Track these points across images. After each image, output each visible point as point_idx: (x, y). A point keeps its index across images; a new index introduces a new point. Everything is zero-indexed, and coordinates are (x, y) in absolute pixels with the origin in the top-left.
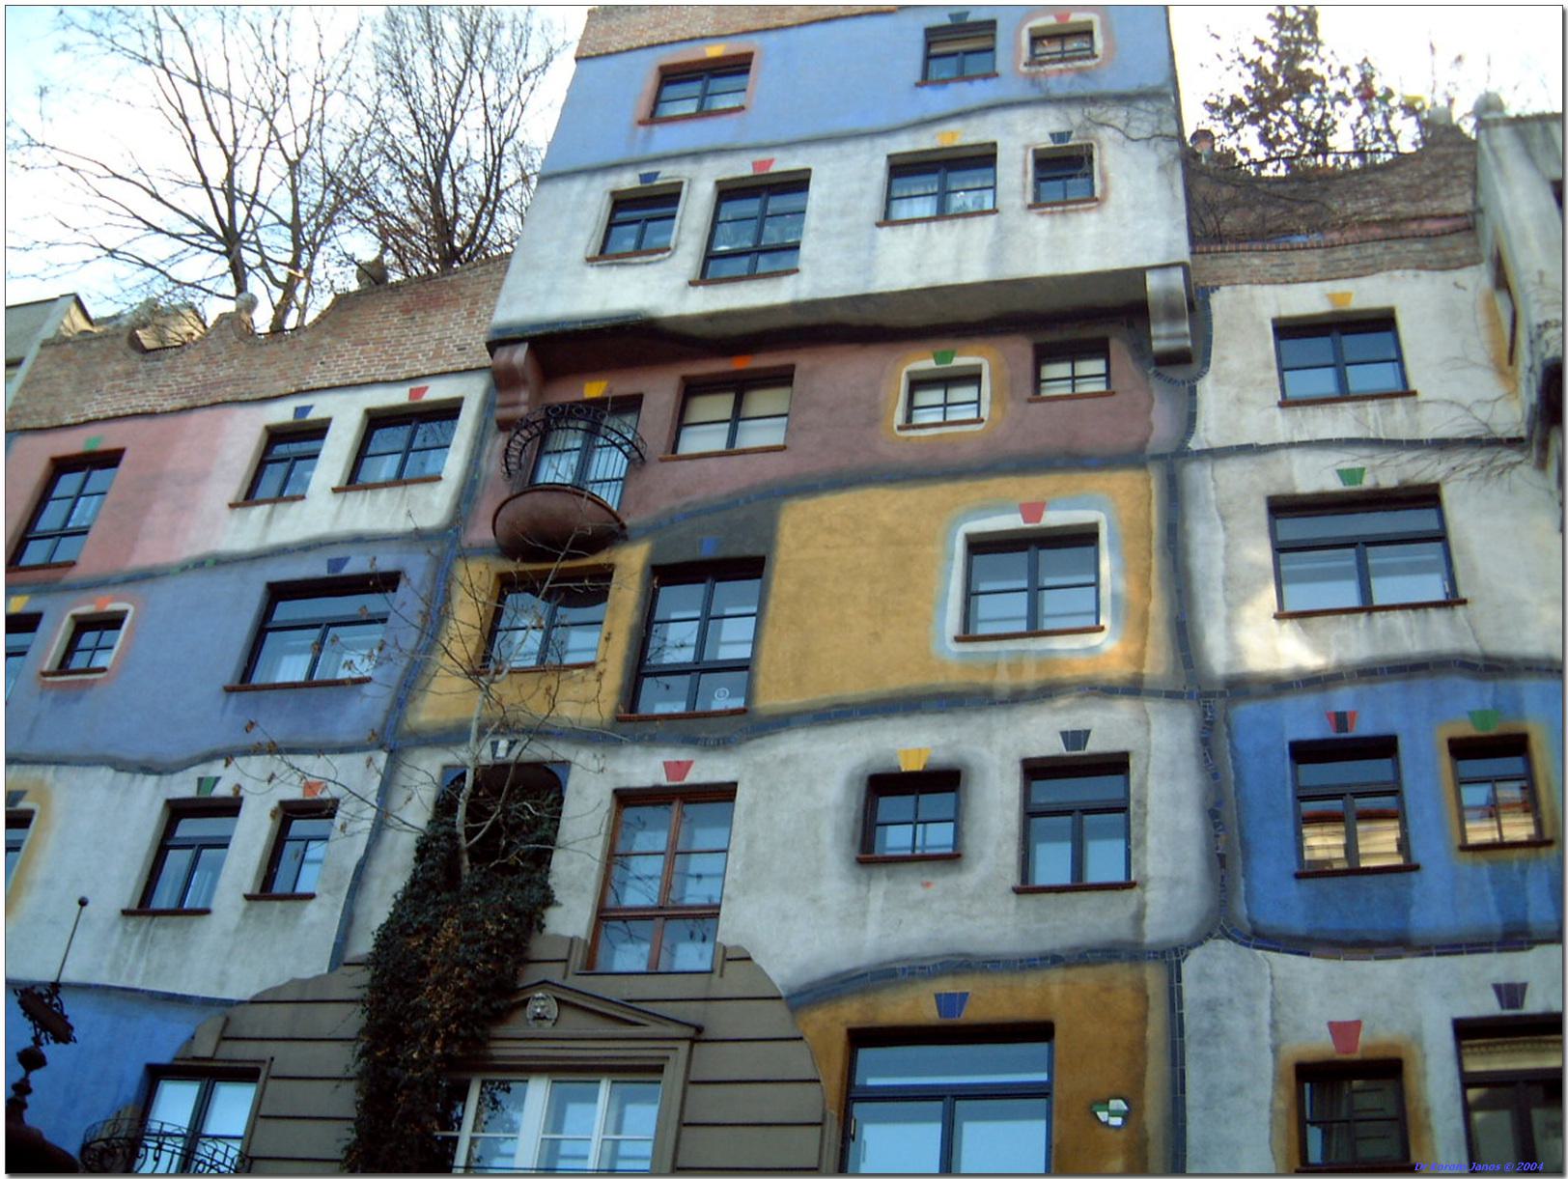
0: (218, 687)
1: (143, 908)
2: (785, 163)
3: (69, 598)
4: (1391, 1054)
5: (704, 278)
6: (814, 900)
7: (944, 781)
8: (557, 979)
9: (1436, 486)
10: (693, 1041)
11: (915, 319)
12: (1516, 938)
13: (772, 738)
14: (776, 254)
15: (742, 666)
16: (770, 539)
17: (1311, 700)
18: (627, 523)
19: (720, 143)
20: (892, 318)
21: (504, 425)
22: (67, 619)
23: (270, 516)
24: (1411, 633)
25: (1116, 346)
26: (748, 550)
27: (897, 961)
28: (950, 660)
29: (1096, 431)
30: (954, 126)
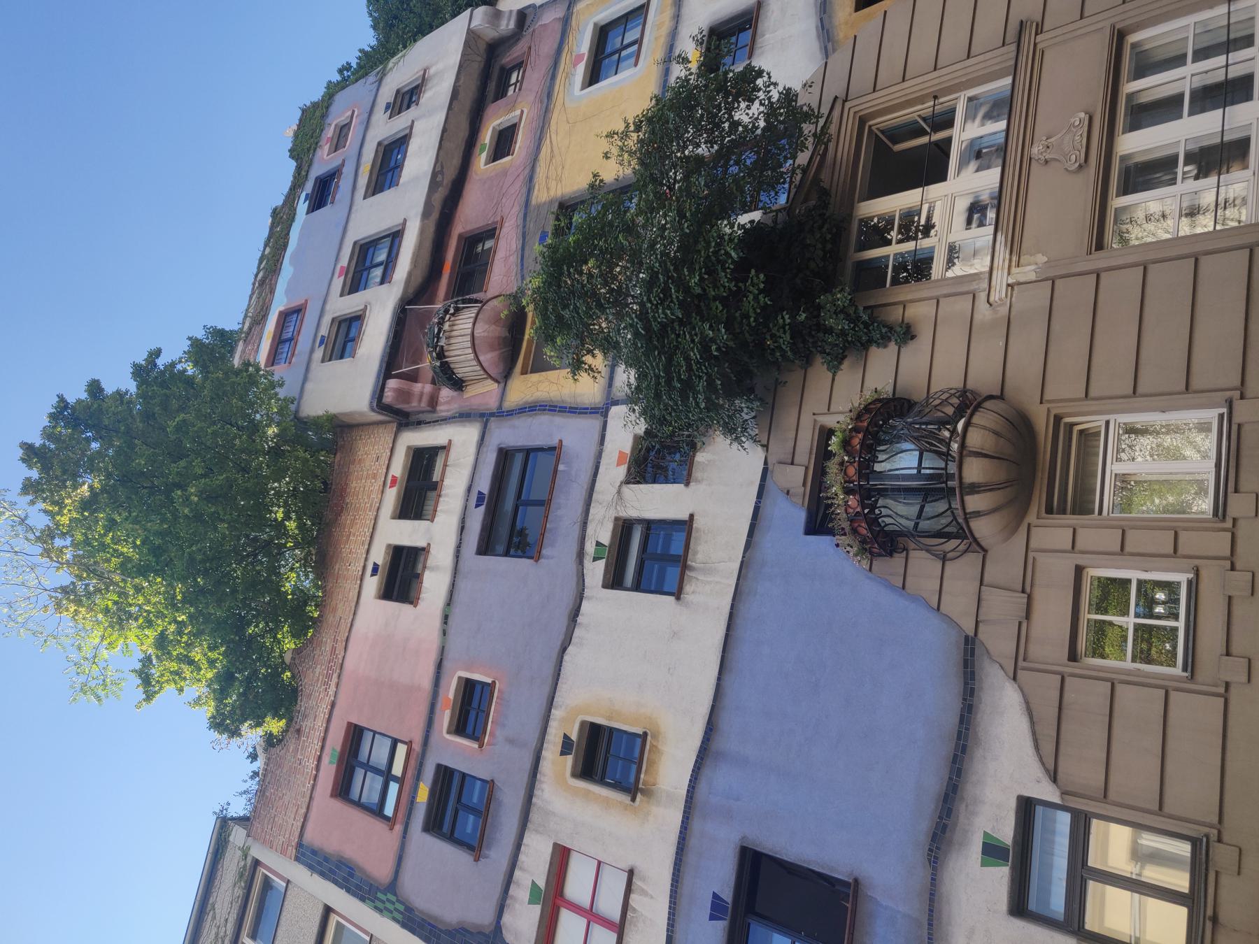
2: (344, 261)
3: (434, 738)
10: (845, 101)
11: (456, 161)
16: (551, 202)
19: (321, 303)
20: (450, 174)
21: (433, 402)
22: (448, 737)
25: (508, 59)
29: (546, 47)
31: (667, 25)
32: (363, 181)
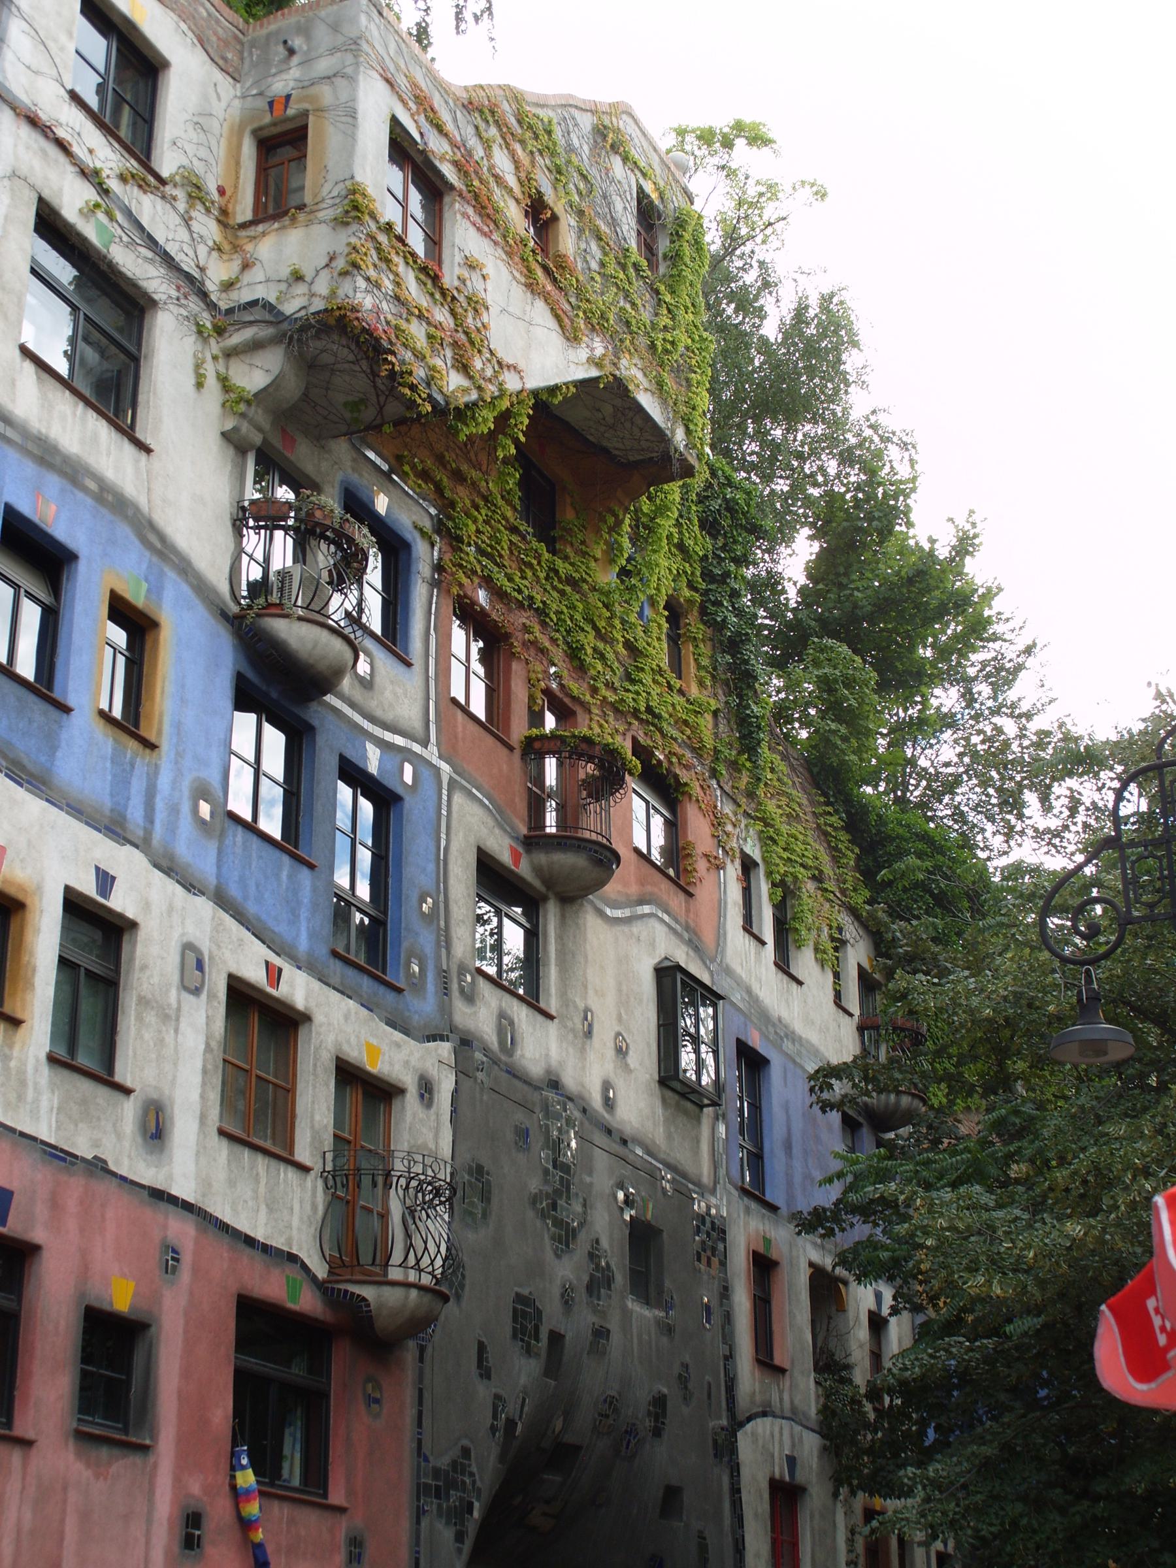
4: (20, 896)
9: (153, 303)
12: (114, 828)
17: (30, 468)
24: (108, 455)
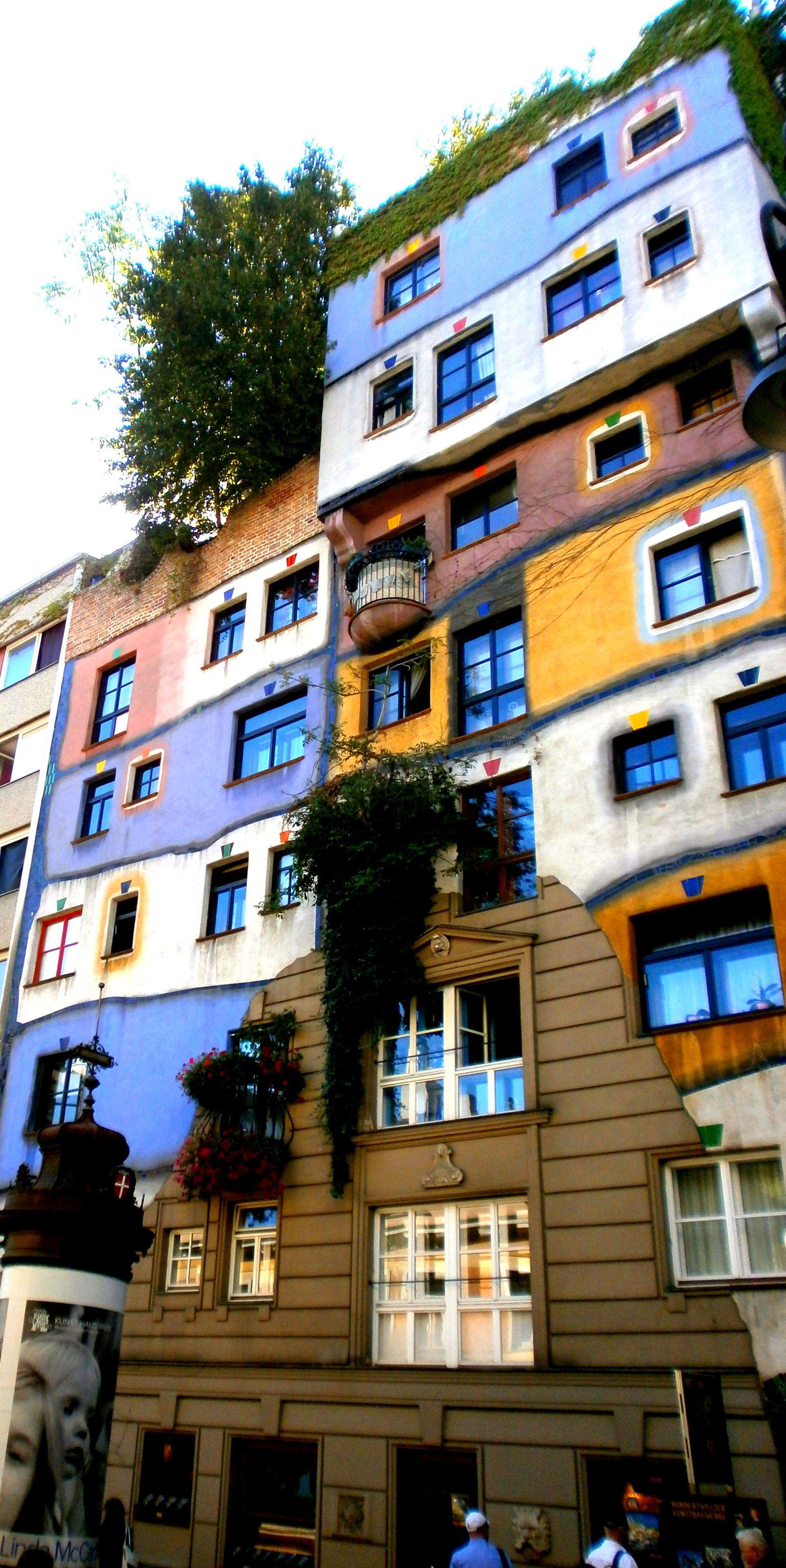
0: (219, 786)
1: (210, 933)
5: (441, 422)
6: (592, 834)
7: (664, 730)
8: (446, 922)
10: (533, 945)
13: (546, 730)
14: (477, 391)
15: (520, 685)
16: (521, 593)
18: (430, 608)
23: (226, 664)
26: (509, 604)
27: (653, 862)
28: (651, 641)
30: (582, 240)
31: (692, 647)
32: (566, 260)
